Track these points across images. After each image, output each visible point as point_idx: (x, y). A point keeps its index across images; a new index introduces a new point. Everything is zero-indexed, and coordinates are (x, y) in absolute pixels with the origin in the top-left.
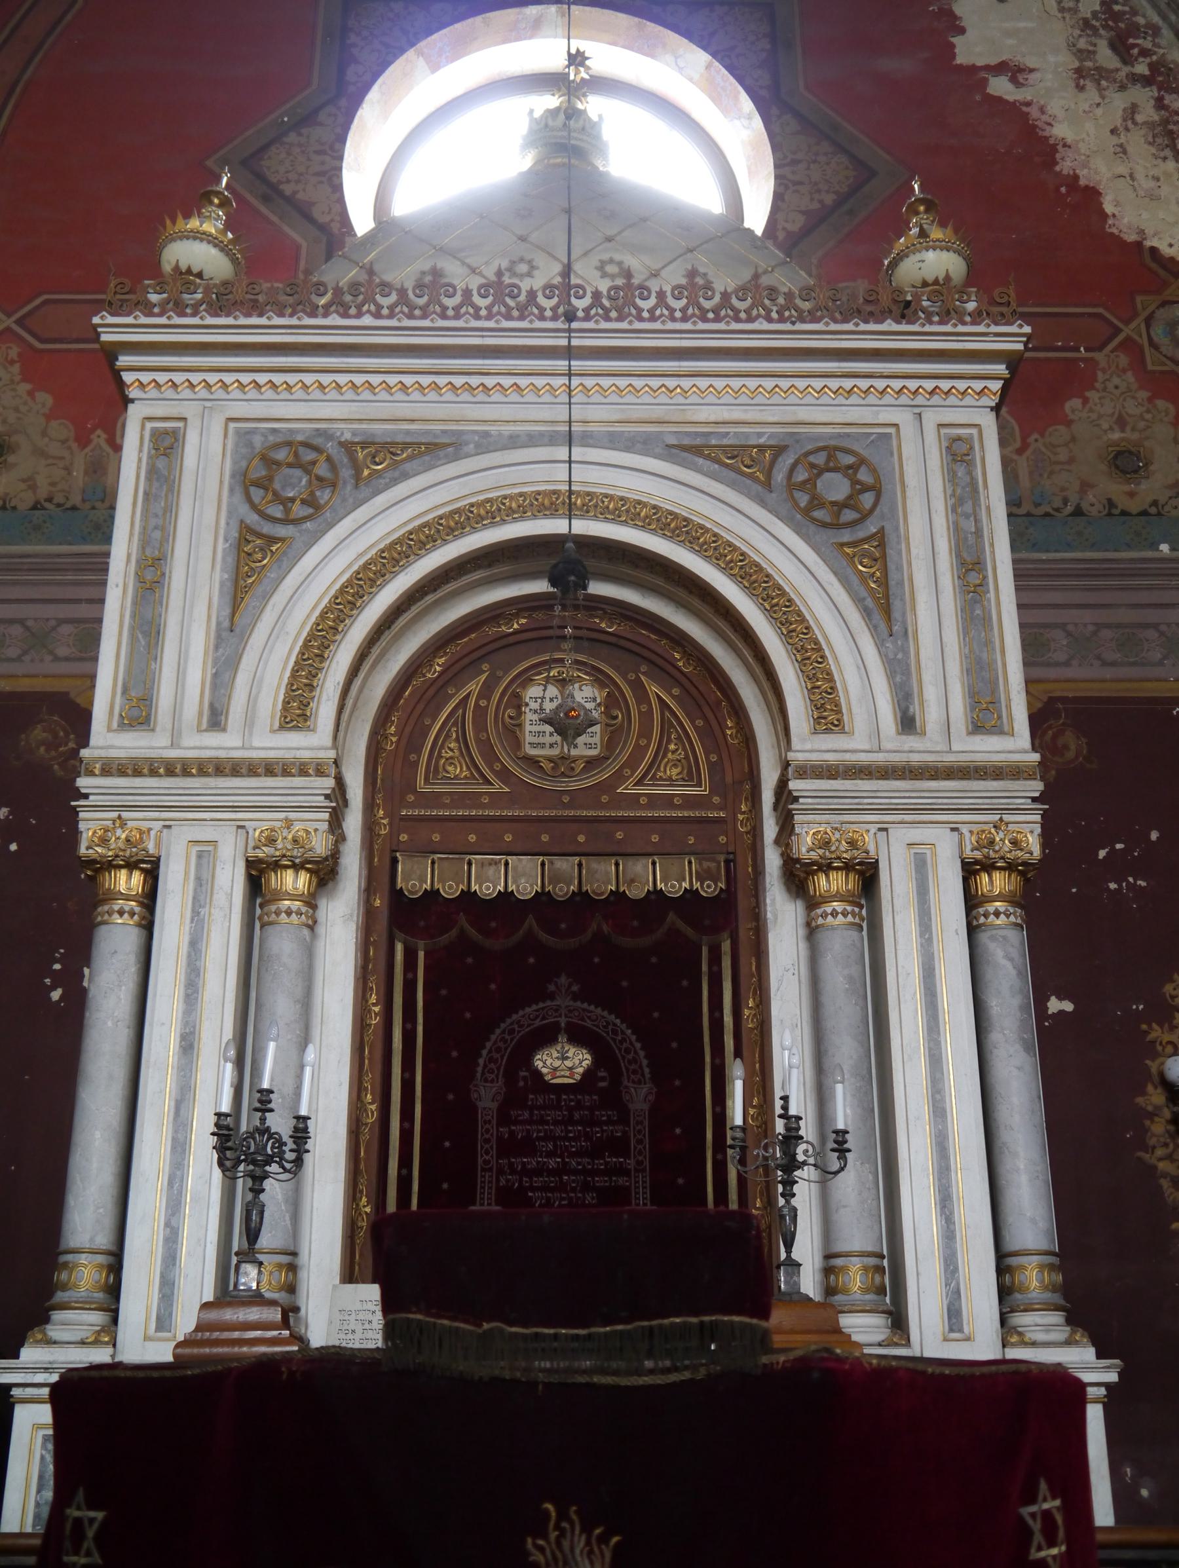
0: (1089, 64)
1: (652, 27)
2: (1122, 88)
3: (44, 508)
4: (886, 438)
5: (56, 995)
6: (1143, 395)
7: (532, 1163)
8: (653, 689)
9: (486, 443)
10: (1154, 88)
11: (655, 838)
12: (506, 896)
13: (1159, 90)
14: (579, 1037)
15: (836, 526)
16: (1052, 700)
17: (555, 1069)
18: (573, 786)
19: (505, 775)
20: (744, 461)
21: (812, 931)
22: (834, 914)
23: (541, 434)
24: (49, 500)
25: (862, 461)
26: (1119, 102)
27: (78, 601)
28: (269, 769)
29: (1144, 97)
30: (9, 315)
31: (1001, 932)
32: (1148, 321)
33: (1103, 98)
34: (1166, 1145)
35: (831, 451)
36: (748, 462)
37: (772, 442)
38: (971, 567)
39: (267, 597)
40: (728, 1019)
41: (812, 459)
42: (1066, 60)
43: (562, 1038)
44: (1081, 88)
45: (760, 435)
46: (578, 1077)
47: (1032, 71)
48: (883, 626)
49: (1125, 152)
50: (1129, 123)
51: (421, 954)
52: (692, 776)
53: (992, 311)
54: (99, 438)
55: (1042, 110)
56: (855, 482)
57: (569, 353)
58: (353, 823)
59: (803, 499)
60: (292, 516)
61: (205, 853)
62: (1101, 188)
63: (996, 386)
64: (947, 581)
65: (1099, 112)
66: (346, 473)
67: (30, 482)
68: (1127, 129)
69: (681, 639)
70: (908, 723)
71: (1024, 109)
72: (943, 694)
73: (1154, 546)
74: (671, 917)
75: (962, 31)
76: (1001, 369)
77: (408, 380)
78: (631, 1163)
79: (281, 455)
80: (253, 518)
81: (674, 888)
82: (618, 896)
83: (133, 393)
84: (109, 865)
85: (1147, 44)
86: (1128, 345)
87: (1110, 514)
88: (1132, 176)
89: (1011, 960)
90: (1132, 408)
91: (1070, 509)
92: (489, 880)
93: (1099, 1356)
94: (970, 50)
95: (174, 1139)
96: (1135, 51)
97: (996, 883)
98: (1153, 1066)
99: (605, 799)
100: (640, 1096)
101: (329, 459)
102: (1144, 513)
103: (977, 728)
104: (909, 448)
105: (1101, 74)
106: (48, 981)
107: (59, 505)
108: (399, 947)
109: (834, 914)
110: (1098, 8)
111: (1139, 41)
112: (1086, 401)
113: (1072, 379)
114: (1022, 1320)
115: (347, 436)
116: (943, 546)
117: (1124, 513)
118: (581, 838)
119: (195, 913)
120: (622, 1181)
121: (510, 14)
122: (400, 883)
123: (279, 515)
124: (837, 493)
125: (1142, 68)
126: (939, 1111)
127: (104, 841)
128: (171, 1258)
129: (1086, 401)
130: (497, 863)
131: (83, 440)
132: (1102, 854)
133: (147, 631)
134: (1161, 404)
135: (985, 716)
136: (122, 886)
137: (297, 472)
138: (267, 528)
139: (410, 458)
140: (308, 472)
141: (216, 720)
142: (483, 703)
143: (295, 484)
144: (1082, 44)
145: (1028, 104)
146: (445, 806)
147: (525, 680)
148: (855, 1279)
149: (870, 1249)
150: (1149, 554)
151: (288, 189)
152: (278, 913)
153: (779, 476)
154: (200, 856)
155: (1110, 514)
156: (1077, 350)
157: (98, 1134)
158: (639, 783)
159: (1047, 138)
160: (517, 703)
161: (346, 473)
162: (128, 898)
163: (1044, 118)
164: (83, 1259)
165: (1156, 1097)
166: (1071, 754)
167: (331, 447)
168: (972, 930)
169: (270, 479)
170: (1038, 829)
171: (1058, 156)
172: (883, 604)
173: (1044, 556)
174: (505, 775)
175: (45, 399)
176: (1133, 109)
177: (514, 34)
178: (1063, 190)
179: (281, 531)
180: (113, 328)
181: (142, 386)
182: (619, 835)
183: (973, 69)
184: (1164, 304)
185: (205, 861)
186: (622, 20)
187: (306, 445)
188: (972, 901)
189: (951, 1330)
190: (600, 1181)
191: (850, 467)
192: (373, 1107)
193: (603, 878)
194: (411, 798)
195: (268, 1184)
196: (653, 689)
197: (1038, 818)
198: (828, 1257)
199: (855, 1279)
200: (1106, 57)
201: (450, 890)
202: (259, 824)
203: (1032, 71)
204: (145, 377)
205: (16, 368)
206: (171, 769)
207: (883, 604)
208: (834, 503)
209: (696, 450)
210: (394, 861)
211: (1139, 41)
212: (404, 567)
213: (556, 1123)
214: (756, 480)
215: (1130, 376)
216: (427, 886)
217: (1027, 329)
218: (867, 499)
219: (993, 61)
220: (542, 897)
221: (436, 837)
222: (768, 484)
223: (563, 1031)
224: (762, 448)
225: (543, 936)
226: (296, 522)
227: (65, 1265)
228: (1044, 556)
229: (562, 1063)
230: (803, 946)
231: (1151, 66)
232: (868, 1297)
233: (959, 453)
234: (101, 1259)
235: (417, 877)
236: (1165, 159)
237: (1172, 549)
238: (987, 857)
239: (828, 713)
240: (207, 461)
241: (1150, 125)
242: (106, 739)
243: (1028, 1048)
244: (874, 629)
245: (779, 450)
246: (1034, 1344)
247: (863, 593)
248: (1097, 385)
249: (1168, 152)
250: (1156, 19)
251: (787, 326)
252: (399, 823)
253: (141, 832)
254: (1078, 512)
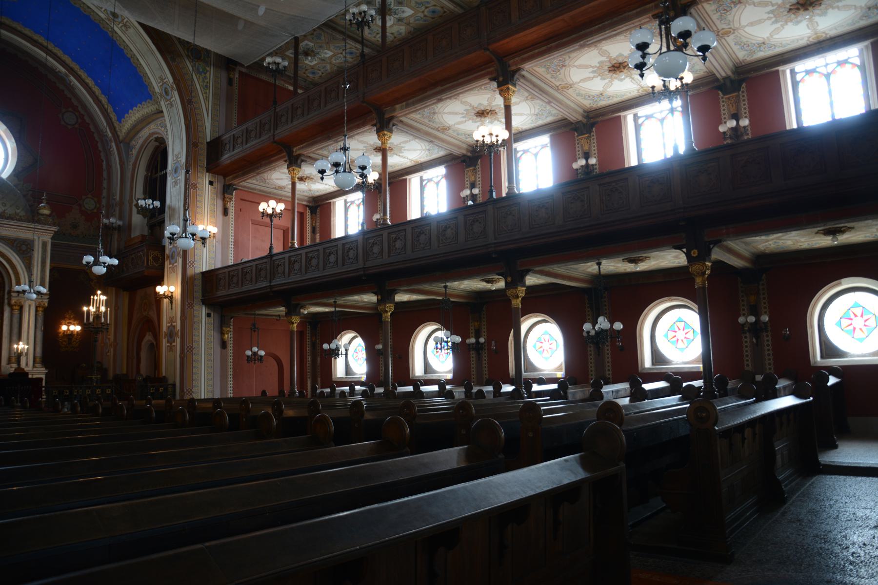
97: (41, 309)
104: (36, 243)
148: (13, 360)
188: (37, 311)
199: (13, 360)
233: (44, 244)
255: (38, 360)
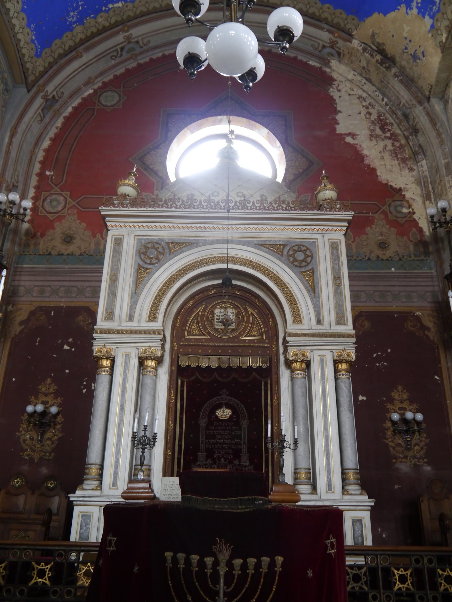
0: (374, 133)
1: (253, 122)
2: (383, 140)
3: (83, 255)
4: (314, 243)
5: (84, 391)
6: (388, 226)
7: (215, 441)
8: (250, 310)
9: (205, 243)
10: (392, 140)
11: (250, 352)
12: (209, 367)
13: (393, 141)
14: (228, 406)
15: (300, 267)
16: (361, 312)
17: (222, 415)
18: (228, 337)
19: (209, 333)
20: (276, 248)
21: (292, 379)
22: (298, 374)
23: (220, 240)
24: (85, 253)
25: (308, 249)
26: (382, 144)
27: (92, 281)
28: (146, 332)
29: (389, 143)
30: (74, 201)
31: (344, 380)
32: (389, 206)
33: (377, 143)
34: (391, 438)
35: (299, 246)
36: (276, 248)
37: (283, 243)
38: (337, 278)
39: (145, 285)
40: (269, 402)
41: (294, 248)
42: (368, 132)
43: (224, 407)
44: (371, 140)
45: (280, 241)
46: (228, 418)
47: (358, 135)
48: (313, 295)
49: (383, 158)
50: (385, 150)
51: (185, 383)
52: (260, 334)
53: (345, 208)
54: (98, 235)
55: (360, 146)
56: (306, 254)
57: (228, 218)
58: (168, 347)
59: (291, 259)
60: (152, 262)
61: (127, 356)
62: (377, 168)
63: (345, 228)
64: (330, 282)
65: (376, 147)
66: (167, 251)
67: (79, 248)
68: (384, 152)
69: (257, 297)
70: (319, 322)
71: (356, 146)
72: (329, 315)
73: (390, 269)
74: (254, 373)
75: (338, 124)
76: (346, 224)
77: (184, 225)
78: (242, 442)
79: (149, 246)
80: (141, 263)
81: (255, 365)
82: (239, 367)
83: (110, 228)
84: (101, 358)
85: (390, 128)
86: (384, 213)
87: (378, 260)
88: (385, 165)
89: (347, 388)
90: (384, 230)
91: (367, 258)
92: (205, 362)
93: (369, 498)
94: (340, 129)
95: (118, 434)
96: (386, 130)
98: (388, 416)
99: (236, 340)
100: (245, 423)
101: (162, 247)
102: (387, 260)
103: (338, 323)
104: (321, 245)
105: (377, 136)
106: (82, 387)
107: (87, 254)
108: (179, 381)
109: (298, 374)
110: (376, 118)
111: (388, 127)
112: (371, 228)
113: (368, 222)
114: (348, 488)
115: (167, 240)
116: (330, 273)
117: (382, 260)
118: (230, 351)
119: (125, 372)
120: (239, 447)
121: (213, 118)
122: (180, 363)
123: (149, 262)
124: (301, 257)
125: (388, 135)
126: (326, 429)
127: (100, 352)
128: (117, 467)
129: (371, 228)
130: (206, 358)
131: (94, 236)
132: (374, 355)
133: (113, 294)
134: (393, 229)
135: (340, 320)
136: (105, 364)
137: (154, 250)
138: (145, 266)
139: (185, 247)
140: (157, 250)
141: (131, 318)
142: (203, 313)
143: (153, 254)
144: (372, 128)
145: (357, 144)
146: (193, 342)
147: (215, 307)
148: (303, 476)
149: (307, 467)
150: (389, 271)
151: (151, 167)
152: (147, 372)
153: (285, 253)
154: (126, 356)
155: (378, 260)
156: (369, 213)
157: (97, 432)
158: (246, 336)
159: (361, 154)
160: (213, 313)
161: (167, 251)
162: (106, 367)
163: (361, 148)
164: (93, 466)
165: (389, 424)
166: (366, 327)
167: (163, 243)
168: (336, 379)
169: (146, 252)
170: (354, 352)
171: (365, 159)
172: (313, 289)
173: (359, 271)
174: (209, 333)
175: (84, 225)
176: (385, 147)
177: (214, 123)
178: (366, 168)
179: (149, 266)
180: (104, 210)
181: (112, 226)
182: (240, 350)
183: (341, 135)
184: (394, 201)
185: (127, 357)
186: (244, 120)
187: (156, 243)
188: (336, 371)
189: (329, 490)
190: (233, 446)
191: (304, 250)
192: (172, 425)
193: (236, 362)
194: (183, 339)
195: (146, 450)
196: (250, 310)
197: (354, 348)
198: (295, 469)
199: (303, 476)
200: (378, 131)
201: (194, 365)
202: (143, 347)
203: (358, 135)
204: (113, 224)
205: (76, 216)
206: (119, 332)
207: (313, 289)
208: (300, 260)
209: (262, 245)
210: (178, 357)
211: (388, 127)
212: (182, 277)
213: (222, 430)
214: (279, 254)
215: (384, 221)
216: (187, 364)
217: (353, 213)
218: (309, 259)
219: (347, 132)
220: (219, 368)
221: (190, 351)
222: (282, 255)
223: (224, 404)
224: (280, 245)
225: (219, 378)
226: (153, 264)
227: (88, 468)
228: (359, 271)
229: (224, 413)
230: (290, 382)
231: (391, 134)
232: (306, 480)
233: (334, 247)
234: (98, 466)
235: (185, 362)
236: (394, 160)
237: (395, 270)
238: (340, 359)
239: (297, 319)
240: (129, 247)
241: (390, 151)
242: (101, 323)
243: (351, 412)
244: (310, 295)
245: (285, 245)
246: (351, 494)
247: (307, 285)
248: (375, 224)
249: (395, 158)
250: (392, 121)
251: (288, 212)
252: (180, 346)
253: (110, 349)
254: (369, 259)
255: (351, 476)
